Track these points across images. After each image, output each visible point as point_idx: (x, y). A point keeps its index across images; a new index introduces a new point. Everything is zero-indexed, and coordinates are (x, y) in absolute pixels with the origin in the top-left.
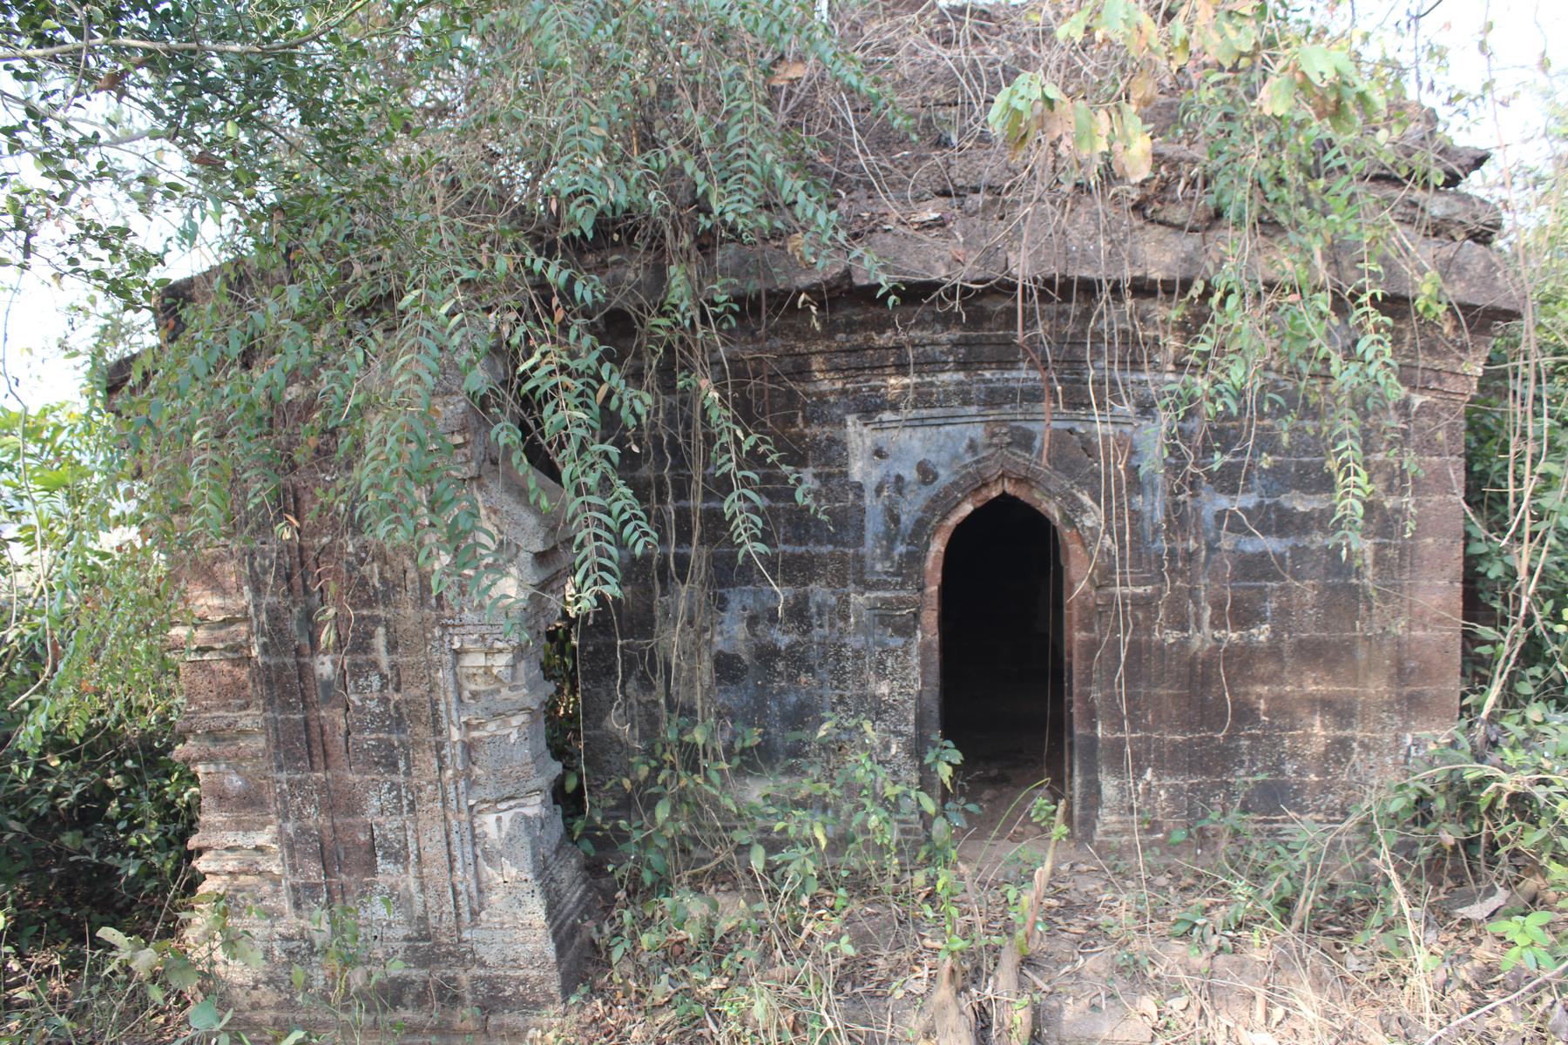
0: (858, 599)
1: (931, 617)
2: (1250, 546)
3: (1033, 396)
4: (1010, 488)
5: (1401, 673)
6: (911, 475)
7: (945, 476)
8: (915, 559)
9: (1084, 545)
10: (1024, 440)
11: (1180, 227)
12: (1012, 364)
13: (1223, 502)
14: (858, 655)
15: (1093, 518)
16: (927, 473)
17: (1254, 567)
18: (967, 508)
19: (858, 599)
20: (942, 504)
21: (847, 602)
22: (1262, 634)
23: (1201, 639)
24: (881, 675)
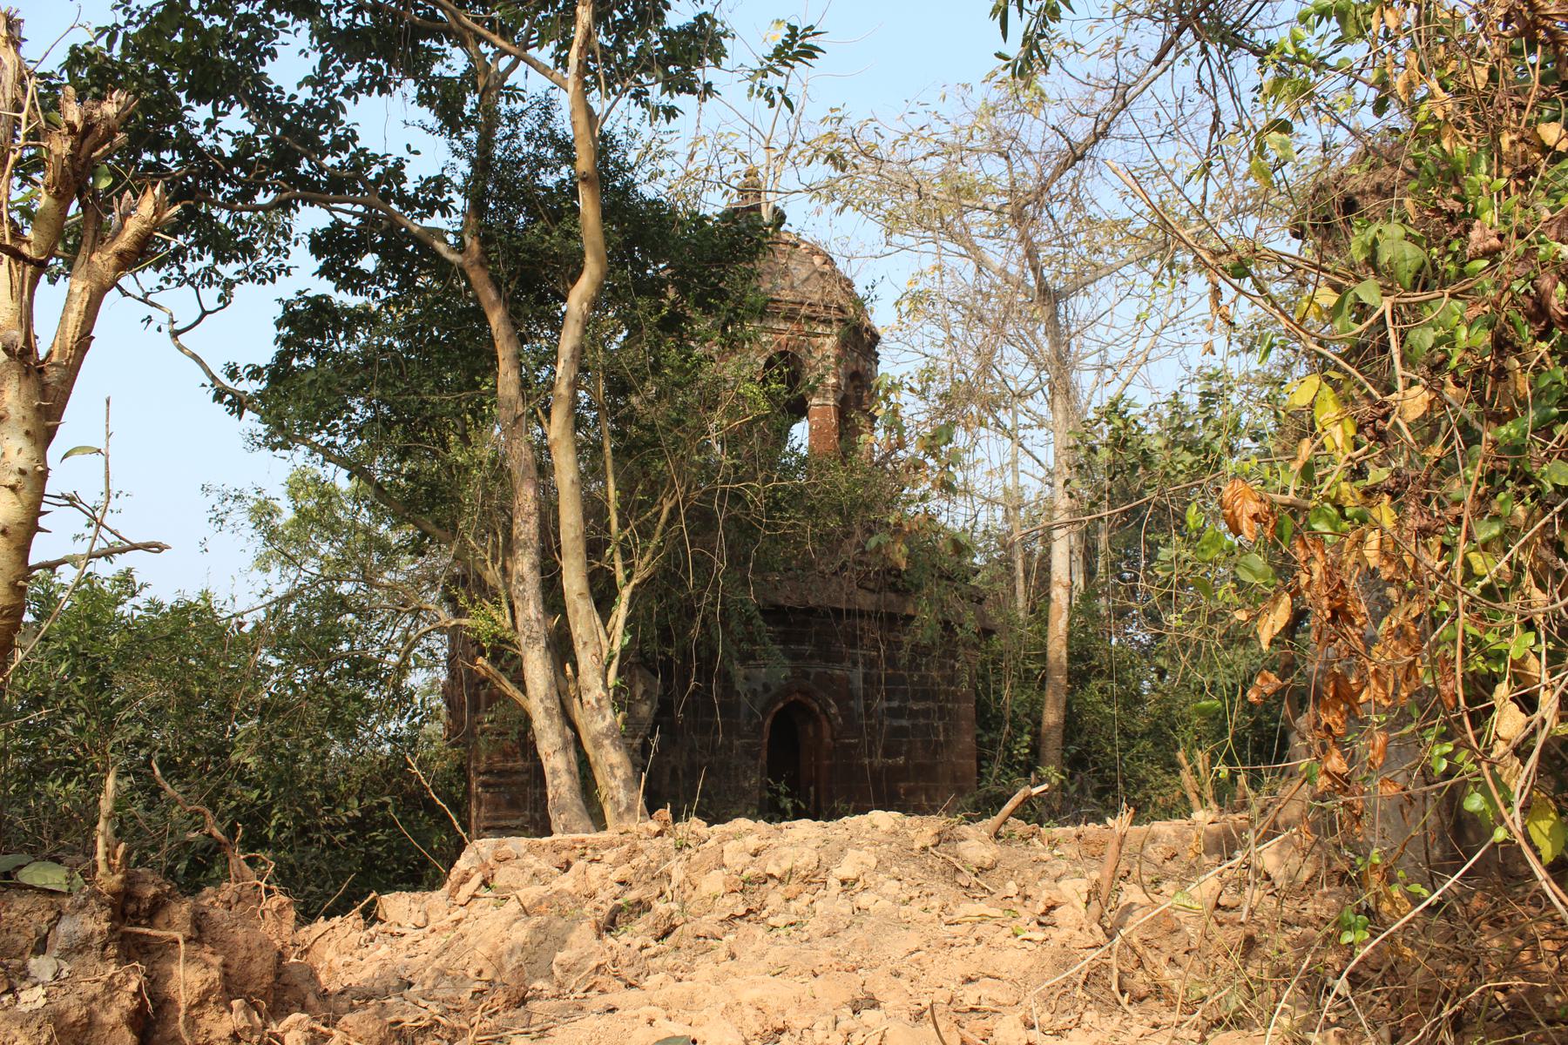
0: (737, 743)
1: (764, 754)
2: (896, 723)
3: (811, 656)
4: (798, 696)
5: (955, 779)
6: (760, 689)
7: (774, 690)
8: (761, 725)
9: (830, 722)
10: (806, 675)
11: (872, 591)
12: (802, 643)
13: (885, 704)
14: (736, 768)
15: (834, 710)
16: (766, 688)
17: (900, 732)
18: (781, 705)
19: (737, 743)
20: (773, 701)
21: (731, 743)
22: (901, 760)
23: (879, 761)
24: (746, 778)
